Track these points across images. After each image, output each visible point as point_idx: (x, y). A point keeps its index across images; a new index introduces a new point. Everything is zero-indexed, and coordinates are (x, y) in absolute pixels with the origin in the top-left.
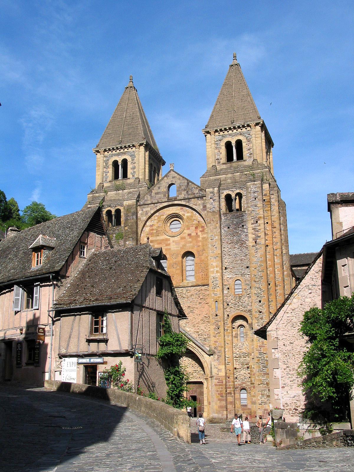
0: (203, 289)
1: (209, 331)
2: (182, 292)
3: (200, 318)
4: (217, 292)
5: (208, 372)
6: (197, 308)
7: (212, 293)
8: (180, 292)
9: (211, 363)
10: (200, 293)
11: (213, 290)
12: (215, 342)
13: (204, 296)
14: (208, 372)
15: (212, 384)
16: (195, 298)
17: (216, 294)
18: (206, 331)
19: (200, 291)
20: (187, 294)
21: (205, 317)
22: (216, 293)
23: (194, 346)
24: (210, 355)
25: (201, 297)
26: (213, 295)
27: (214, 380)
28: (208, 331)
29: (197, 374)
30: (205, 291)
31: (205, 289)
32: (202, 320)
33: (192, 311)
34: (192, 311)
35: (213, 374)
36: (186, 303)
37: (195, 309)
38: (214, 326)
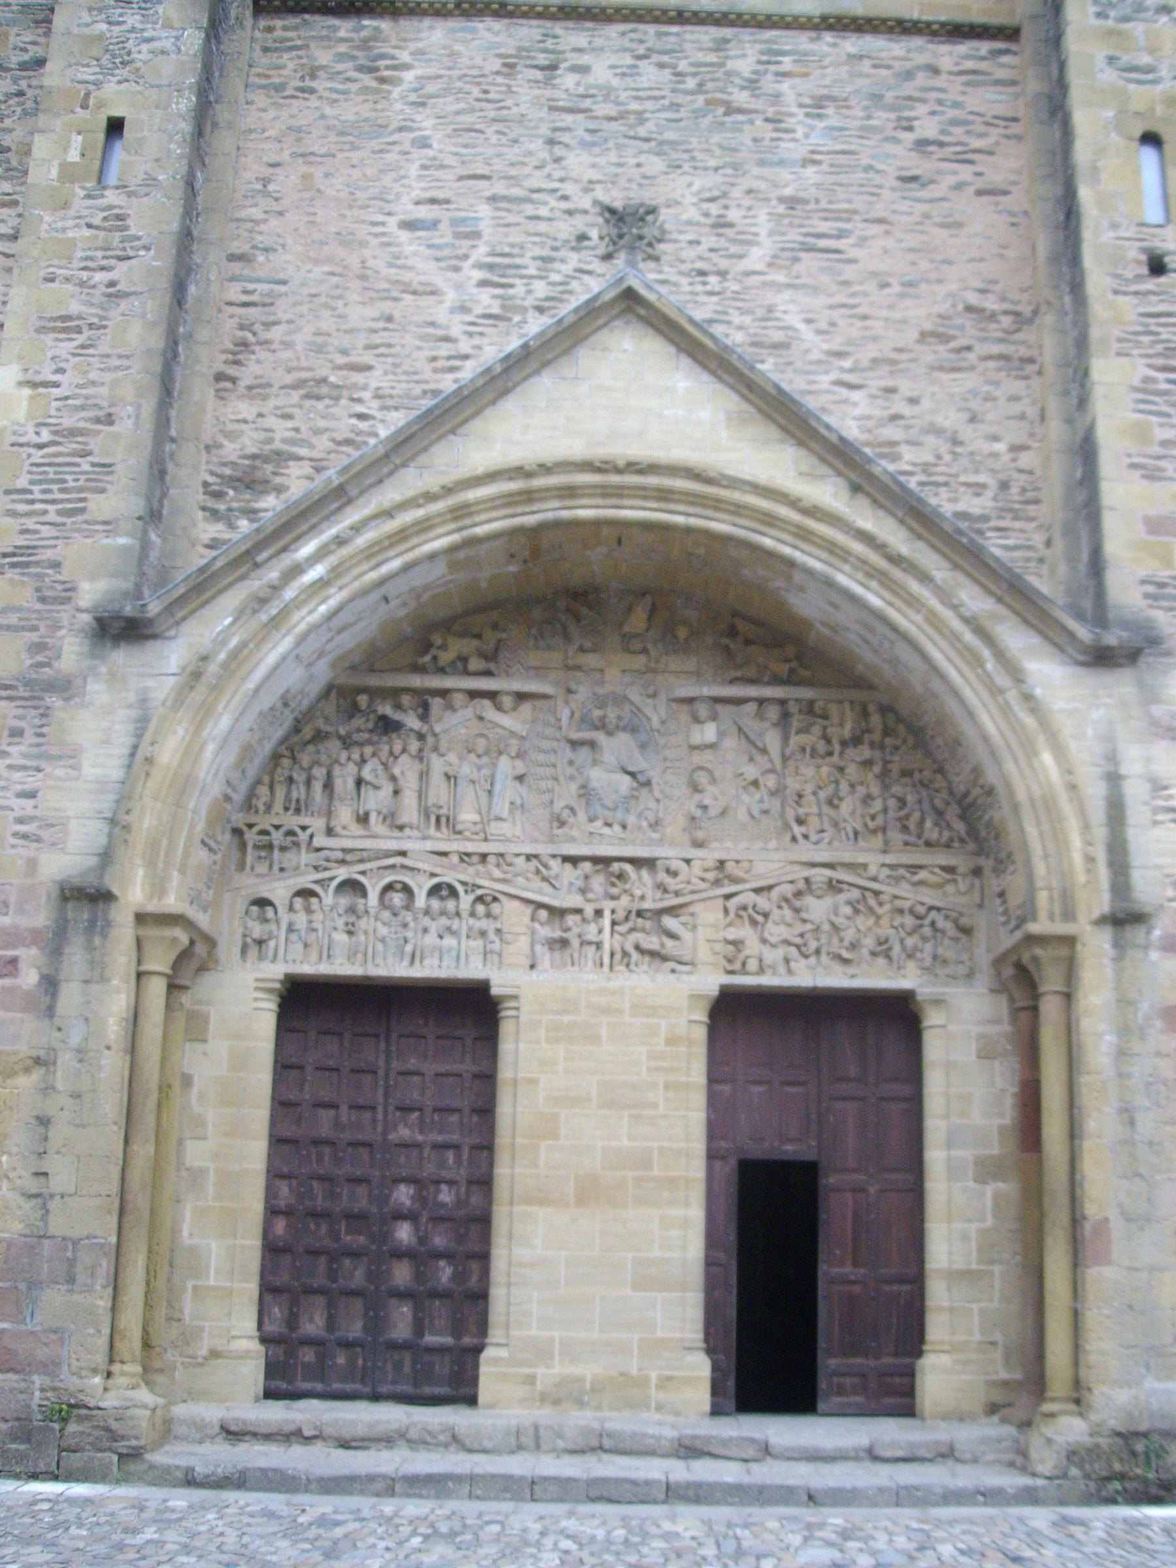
0: (946, 63)
1: (1016, 449)
2: (712, 58)
3: (921, 312)
4: (1151, 51)
5: (1077, 858)
6: (880, 221)
7: (1100, 60)
8: (700, 57)
9: (1112, 758)
10: (909, 89)
11: (1119, 33)
12: (1155, 526)
13: (955, 122)
14: (1077, 858)
15: (1125, 1002)
16: (862, 128)
17: (1143, 73)
18: (987, 447)
19: (909, 75)
20: (768, 84)
21: (969, 309)
22: (1145, 59)
23: (904, 550)
24: (1102, 658)
25: (928, 128)
26: (1109, 76)
27: (1154, 955)
28: (1000, 447)
29: (848, 910)
30: (968, 84)
31: (970, 65)
32: (943, 338)
33: (823, 243)
34: (823, 243)
35: (1146, 887)
36: (761, 163)
37: (858, 227)
38: (1139, 370)
